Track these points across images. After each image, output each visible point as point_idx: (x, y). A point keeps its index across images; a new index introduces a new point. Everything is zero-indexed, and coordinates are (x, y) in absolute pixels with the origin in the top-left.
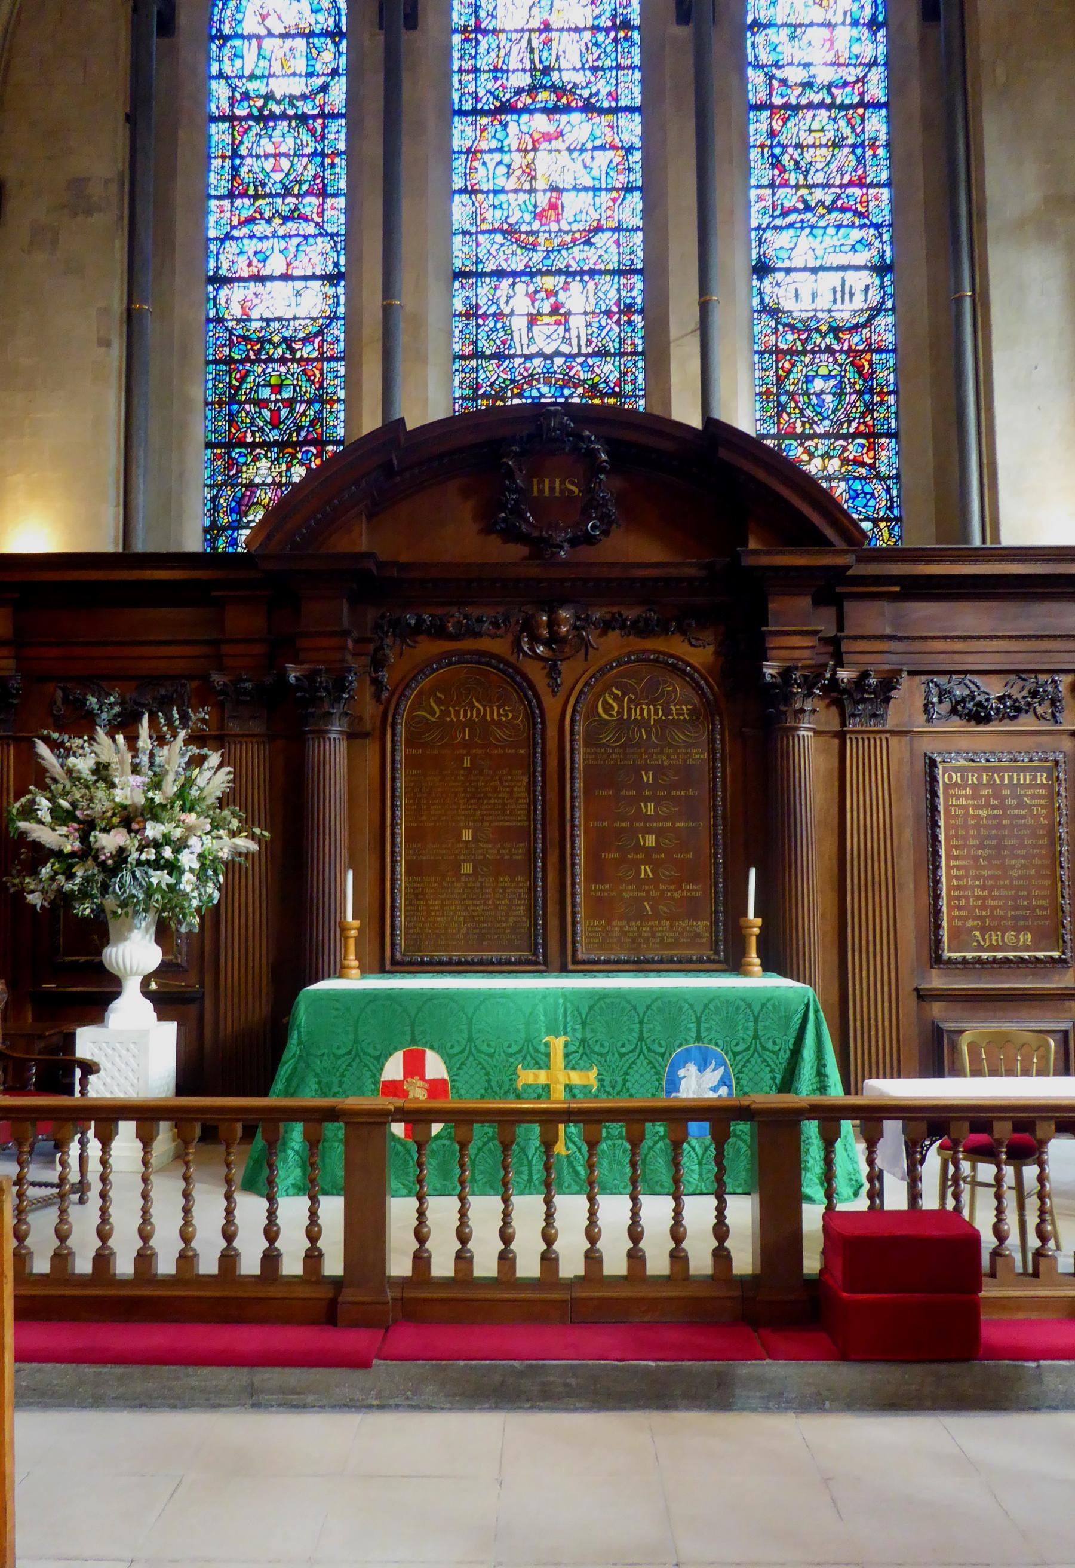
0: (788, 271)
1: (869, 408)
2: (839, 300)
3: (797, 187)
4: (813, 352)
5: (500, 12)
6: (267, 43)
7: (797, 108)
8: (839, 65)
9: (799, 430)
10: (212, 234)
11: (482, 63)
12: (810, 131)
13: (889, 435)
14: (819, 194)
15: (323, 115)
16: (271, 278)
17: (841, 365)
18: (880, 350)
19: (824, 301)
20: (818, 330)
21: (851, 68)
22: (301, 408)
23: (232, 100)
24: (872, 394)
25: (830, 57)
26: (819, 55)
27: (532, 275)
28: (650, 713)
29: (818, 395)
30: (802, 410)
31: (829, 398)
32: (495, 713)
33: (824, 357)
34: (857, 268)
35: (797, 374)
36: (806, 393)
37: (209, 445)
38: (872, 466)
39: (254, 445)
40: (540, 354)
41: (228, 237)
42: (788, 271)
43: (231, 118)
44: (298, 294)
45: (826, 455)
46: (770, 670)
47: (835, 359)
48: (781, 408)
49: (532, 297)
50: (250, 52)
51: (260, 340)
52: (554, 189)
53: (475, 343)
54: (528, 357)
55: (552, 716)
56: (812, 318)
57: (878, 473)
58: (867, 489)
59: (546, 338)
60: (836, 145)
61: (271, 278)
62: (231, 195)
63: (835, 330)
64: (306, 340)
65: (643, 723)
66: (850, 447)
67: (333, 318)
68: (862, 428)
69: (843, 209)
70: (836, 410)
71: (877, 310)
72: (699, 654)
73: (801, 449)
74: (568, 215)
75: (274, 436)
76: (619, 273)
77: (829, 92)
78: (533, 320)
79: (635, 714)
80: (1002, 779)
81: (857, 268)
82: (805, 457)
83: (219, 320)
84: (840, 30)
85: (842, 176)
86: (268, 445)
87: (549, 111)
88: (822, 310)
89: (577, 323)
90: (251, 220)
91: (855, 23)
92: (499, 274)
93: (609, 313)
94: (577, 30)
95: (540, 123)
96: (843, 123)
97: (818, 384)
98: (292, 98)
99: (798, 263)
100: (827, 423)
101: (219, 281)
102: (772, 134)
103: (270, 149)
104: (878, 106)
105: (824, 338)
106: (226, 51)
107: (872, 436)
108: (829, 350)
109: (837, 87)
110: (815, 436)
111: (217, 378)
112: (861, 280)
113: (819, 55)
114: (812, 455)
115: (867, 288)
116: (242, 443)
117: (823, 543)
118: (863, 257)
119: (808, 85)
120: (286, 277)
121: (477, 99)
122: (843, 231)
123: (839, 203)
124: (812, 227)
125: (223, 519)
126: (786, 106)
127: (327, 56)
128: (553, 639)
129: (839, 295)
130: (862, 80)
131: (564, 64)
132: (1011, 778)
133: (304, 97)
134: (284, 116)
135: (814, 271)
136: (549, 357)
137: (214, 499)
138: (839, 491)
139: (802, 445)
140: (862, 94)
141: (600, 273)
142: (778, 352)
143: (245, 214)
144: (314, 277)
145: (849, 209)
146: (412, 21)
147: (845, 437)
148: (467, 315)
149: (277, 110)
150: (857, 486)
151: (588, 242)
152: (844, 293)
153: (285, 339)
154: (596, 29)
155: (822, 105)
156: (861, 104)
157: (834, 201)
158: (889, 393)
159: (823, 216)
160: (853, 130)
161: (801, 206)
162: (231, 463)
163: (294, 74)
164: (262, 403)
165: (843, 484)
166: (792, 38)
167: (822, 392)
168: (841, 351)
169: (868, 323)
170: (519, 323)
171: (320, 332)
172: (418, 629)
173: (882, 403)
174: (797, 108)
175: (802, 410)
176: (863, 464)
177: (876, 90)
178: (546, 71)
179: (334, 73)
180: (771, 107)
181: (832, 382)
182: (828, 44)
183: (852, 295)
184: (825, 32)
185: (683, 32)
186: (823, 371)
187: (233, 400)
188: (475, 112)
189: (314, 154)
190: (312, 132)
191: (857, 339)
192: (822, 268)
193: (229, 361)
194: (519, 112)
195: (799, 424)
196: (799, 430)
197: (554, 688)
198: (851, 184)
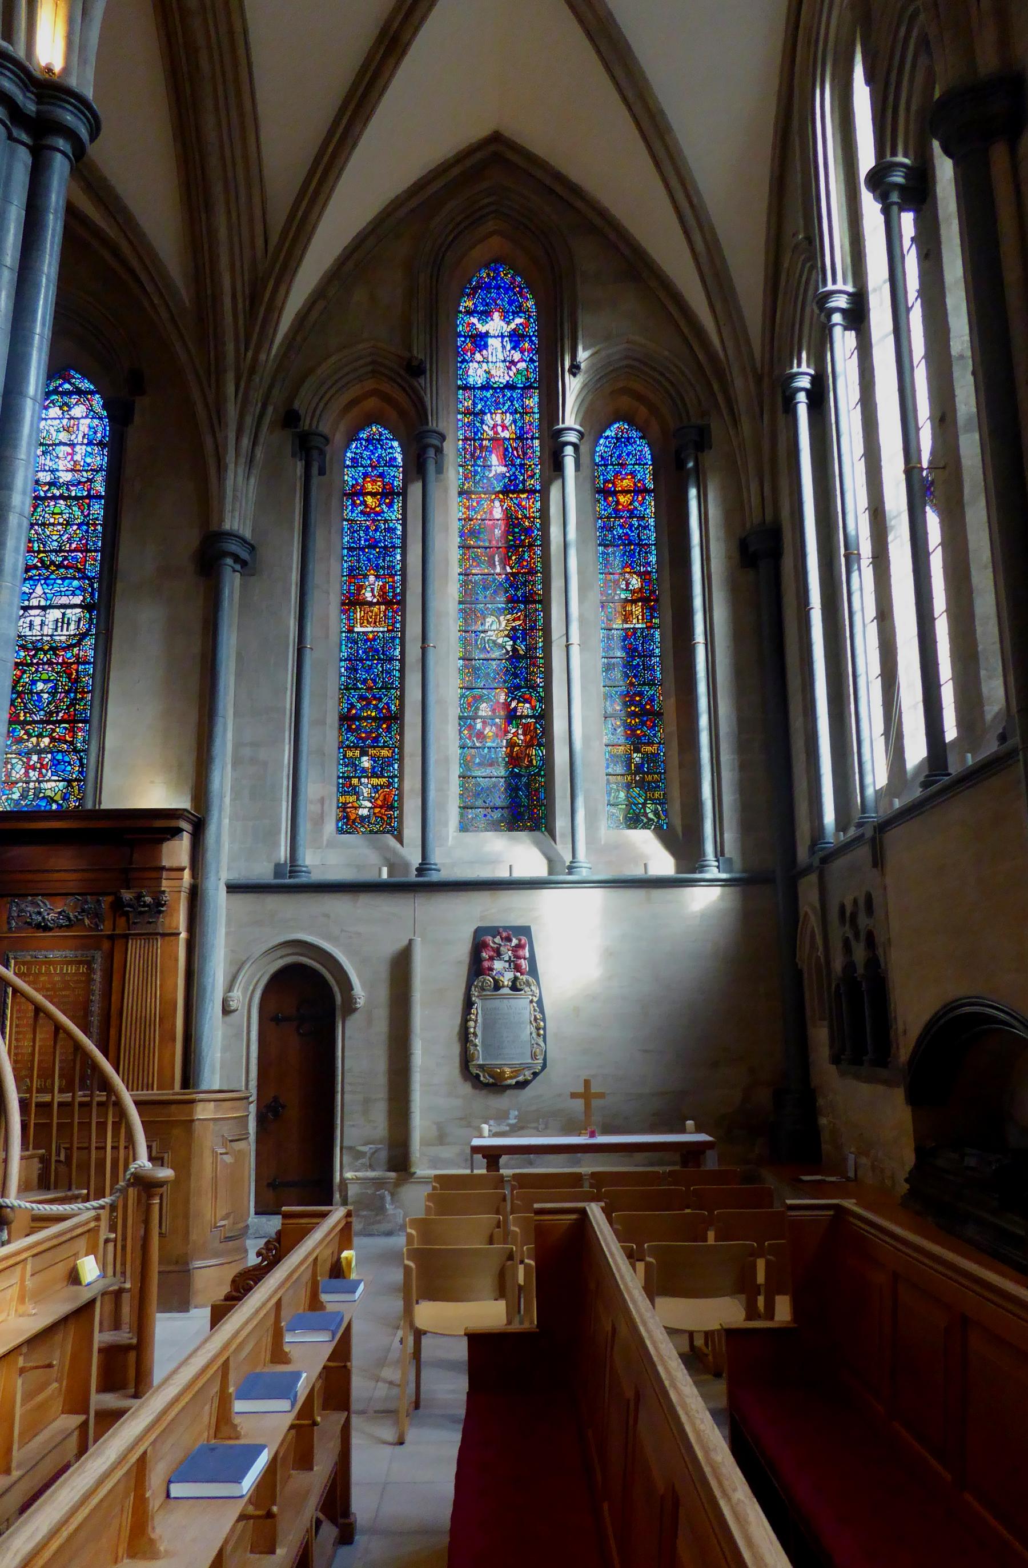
1: (72, 704)
2: (59, 629)
3: (39, 552)
4: (38, 664)
7: (46, 498)
8: (76, 471)
9: (22, 718)
12: (53, 514)
13: (85, 721)
17: (57, 673)
18: (84, 663)
19: (46, 630)
20: (42, 649)
21: (84, 473)
24: (76, 693)
25: (70, 466)
29: (38, 694)
30: (25, 704)
31: (46, 696)
33: (46, 667)
35: (26, 678)
36: (31, 692)
38: (72, 743)
45: (40, 736)
47: (53, 669)
56: (38, 641)
57: (75, 748)
58: (67, 759)
60: (68, 523)
63: (54, 649)
66: (58, 730)
68: (66, 717)
69: (67, 568)
70: (49, 703)
71: (83, 636)
73: (23, 732)
77: (68, 489)
80: (55, 970)
82: (25, 737)
84: (78, 448)
85: (71, 544)
88: (47, 635)
91: (90, 443)
96: (75, 509)
97: (40, 686)
99: (34, 602)
100: (42, 713)
104: (100, 497)
105: (45, 654)
108: (50, 663)
109: (73, 485)
110: (34, 722)
112: (73, 614)
113: (62, 465)
114: (30, 736)
115: (80, 619)
118: (77, 600)
119: (51, 484)
122: (67, 582)
123: (66, 563)
124: (47, 578)
129: (60, 624)
130: (89, 480)
132: (62, 969)
135: (44, 608)
138: (47, 760)
139: (23, 729)
140: (89, 490)
145: (71, 568)
147: (53, 723)
150: (59, 757)
152: (64, 621)
155: (61, 497)
156: (89, 497)
157: (62, 562)
158: (87, 692)
159: (53, 571)
160: (82, 512)
161: (39, 564)
165: (49, 756)
167: (42, 691)
168: (57, 664)
169: (78, 644)
173: (82, 699)
174: (46, 498)
175: (25, 704)
176: (66, 742)
177: (99, 487)
181: (51, 685)
182: (69, 457)
183: (68, 624)
184: (69, 449)
186: (45, 677)
191: (69, 655)
192: (51, 607)
195: (22, 714)
196: (22, 718)
198: (76, 550)
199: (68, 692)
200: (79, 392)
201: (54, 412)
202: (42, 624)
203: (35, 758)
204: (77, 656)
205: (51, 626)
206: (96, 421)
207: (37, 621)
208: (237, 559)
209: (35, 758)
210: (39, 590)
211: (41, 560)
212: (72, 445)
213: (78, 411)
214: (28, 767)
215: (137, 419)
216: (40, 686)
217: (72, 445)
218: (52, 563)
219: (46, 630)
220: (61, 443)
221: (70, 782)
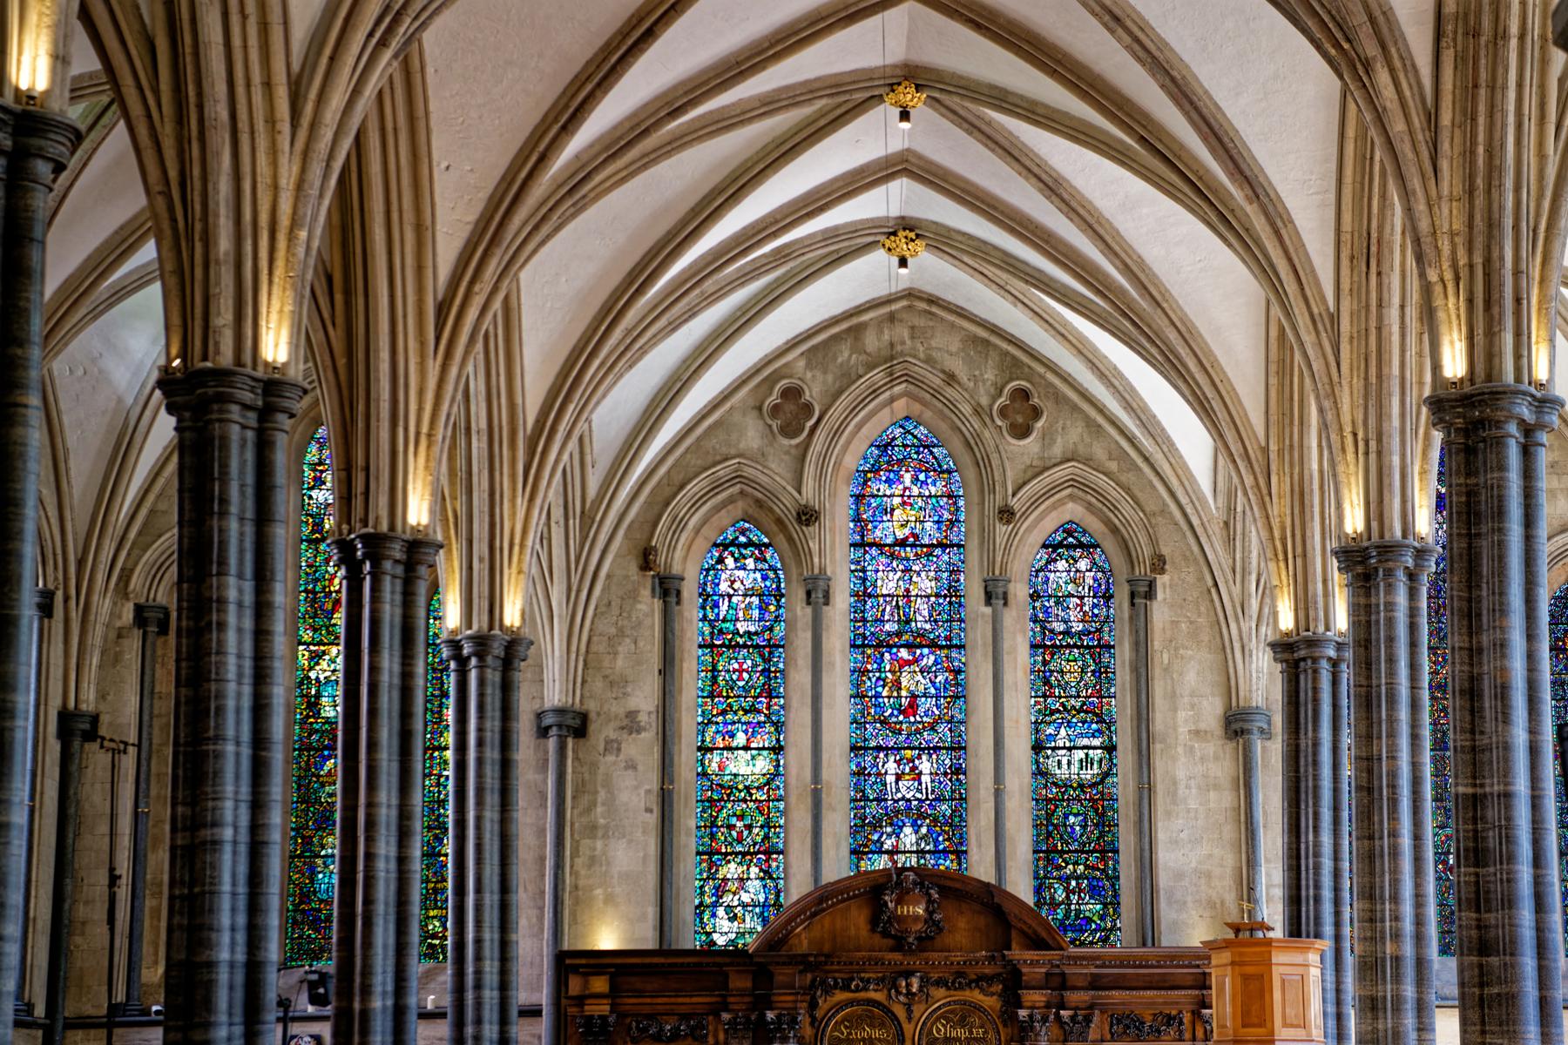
0: (1054, 749)
5: (879, 583)
6: (734, 599)
10: (700, 719)
11: (868, 616)
14: (1073, 701)
15: (769, 646)
16: (737, 748)
22: (756, 831)
23: (712, 633)
26: (1074, 615)
27: (899, 749)
28: (961, 1033)
32: (876, 1034)
34: (1095, 748)
37: (698, 853)
39: (726, 854)
40: (903, 798)
41: (710, 722)
42: (1054, 749)
43: (712, 646)
44: (753, 758)
45: (1076, 863)
46: (1023, 1013)
48: (1049, 834)
49: (898, 762)
50: (724, 607)
51: (730, 787)
52: (914, 697)
53: (863, 791)
54: (896, 801)
55: (908, 1035)
59: (907, 789)
61: (737, 748)
62: (711, 696)
63: (1081, 786)
64: (758, 788)
65: (958, 1039)
67: (777, 774)
69: (1086, 712)
71: (1106, 775)
72: (990, 1002)
74: (921, 711)
75: (739, 848)
76: (953, 749)
78: (898, 777)
79: (954, 1034)
81: (1095, 748)
83: (704, 774)
86: (737, 854)
87: (910, 646)
89: (925, 779)
90: (723, 713)
92: (879, 748)
93: (946, 774)
94: (928, 597)
95: (904, 654)
97: (1072, 819)
98: (749, 633)
101: (704, 749)
102: (1045, 663)
103: (736, 666)
106: (710, 604)
107: (1103, 852)
111: (704, 811)
112: (1096, 754)
113: (1074, 615)
116: (718, 852)
117: (1049, 948)
118: (1096, 742)
119: (1067, 633)
120: (746, 748)
121: (865, 638)
125: (708, 901)
126: (1054, 646)
127: (772, 608)
128: (909, 994)
130: (1098, 630)
131: (919, 618)
133: (756, 633)
134: (745, 646)
135: (1070, 749)
136: (909, 800)
137: (702, 887)
141: (940, 748)
142: (1049, 800)
143: (721, 707)
144: (764, 748)
146: (827, 604)
148: (858, 774)
149: (741, 641)
151: (933, 729)
152: (1086, 762)
153: (747, 788)
154: (937, 596)
155: (1075, 646)
162: (711, 864)
163: (750, 619)
164: (731, 827)
166: (1057, 603)
170: (890, 779)
171: (768, 783)
172: (836, 986)
178: (908, 622)
179: (777, 619)
180: (1045, 647)
185: (988, 610)
187: (713, 825)
188: (863, 646)
189: (763, 671)
190: (762, 656)
193: (710, 800)
194: (890, 647)
197: (910, 1019)
199: (1097, 825)
200: (1081, 545)
201: (1062, 565)
202: (1069, 763)
203: (1073, 883)
204: (1102, 793)
205: (1077, 765)
206: (1100, 575)
207: (1065, 761)
208: (1262, 731)
209: (1073, 883)
210: (1063, 732)
211: (1062, 704)
212: (1081, 598)
213: (1083, 565)
214: (1067, 890)
215: (1160, 595)
216: (1072, 819)
217: (1081, 598)
218: (1073, 707)
219: (1075, 769)
220: (1071, 595)
221: (1105, 905)
